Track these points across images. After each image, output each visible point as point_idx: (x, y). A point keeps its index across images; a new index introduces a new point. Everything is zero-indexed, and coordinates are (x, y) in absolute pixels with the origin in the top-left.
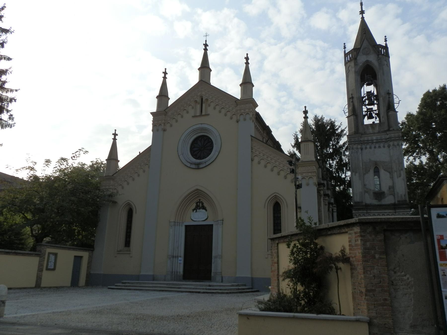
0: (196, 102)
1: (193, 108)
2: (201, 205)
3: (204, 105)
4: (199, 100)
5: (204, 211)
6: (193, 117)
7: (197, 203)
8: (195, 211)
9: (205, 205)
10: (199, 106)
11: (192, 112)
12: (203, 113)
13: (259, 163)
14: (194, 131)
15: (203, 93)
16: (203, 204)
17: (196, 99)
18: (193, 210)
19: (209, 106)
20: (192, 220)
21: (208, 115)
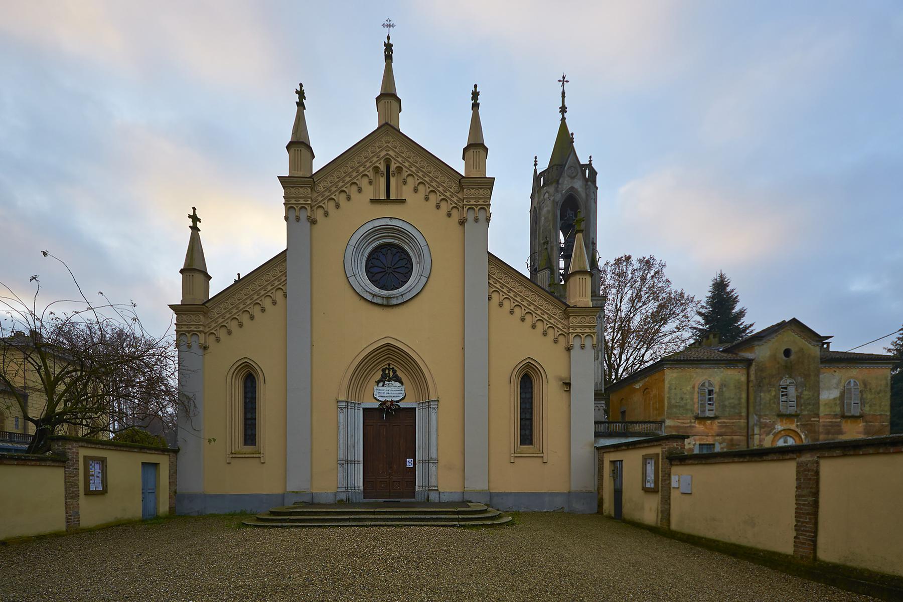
0: (376, 169)
1: (371, 183)
2: (391, 374)
3: (393, 181)
4: (382, 168)
5: (398, 384)
6: (373, 201)
7: (384, 371)
8: (381, 384)
9: (399, 373)
10: (383, 181)
11: (369, 192)
12: (393, 197)
13: (501, 305)
14: (376, 230)
15: (391, 153)
16: (394, 372)
17: (377, 164)
18: (378, 383)
19: (405, 182)
20: (376, 399)
21: (403, 201)
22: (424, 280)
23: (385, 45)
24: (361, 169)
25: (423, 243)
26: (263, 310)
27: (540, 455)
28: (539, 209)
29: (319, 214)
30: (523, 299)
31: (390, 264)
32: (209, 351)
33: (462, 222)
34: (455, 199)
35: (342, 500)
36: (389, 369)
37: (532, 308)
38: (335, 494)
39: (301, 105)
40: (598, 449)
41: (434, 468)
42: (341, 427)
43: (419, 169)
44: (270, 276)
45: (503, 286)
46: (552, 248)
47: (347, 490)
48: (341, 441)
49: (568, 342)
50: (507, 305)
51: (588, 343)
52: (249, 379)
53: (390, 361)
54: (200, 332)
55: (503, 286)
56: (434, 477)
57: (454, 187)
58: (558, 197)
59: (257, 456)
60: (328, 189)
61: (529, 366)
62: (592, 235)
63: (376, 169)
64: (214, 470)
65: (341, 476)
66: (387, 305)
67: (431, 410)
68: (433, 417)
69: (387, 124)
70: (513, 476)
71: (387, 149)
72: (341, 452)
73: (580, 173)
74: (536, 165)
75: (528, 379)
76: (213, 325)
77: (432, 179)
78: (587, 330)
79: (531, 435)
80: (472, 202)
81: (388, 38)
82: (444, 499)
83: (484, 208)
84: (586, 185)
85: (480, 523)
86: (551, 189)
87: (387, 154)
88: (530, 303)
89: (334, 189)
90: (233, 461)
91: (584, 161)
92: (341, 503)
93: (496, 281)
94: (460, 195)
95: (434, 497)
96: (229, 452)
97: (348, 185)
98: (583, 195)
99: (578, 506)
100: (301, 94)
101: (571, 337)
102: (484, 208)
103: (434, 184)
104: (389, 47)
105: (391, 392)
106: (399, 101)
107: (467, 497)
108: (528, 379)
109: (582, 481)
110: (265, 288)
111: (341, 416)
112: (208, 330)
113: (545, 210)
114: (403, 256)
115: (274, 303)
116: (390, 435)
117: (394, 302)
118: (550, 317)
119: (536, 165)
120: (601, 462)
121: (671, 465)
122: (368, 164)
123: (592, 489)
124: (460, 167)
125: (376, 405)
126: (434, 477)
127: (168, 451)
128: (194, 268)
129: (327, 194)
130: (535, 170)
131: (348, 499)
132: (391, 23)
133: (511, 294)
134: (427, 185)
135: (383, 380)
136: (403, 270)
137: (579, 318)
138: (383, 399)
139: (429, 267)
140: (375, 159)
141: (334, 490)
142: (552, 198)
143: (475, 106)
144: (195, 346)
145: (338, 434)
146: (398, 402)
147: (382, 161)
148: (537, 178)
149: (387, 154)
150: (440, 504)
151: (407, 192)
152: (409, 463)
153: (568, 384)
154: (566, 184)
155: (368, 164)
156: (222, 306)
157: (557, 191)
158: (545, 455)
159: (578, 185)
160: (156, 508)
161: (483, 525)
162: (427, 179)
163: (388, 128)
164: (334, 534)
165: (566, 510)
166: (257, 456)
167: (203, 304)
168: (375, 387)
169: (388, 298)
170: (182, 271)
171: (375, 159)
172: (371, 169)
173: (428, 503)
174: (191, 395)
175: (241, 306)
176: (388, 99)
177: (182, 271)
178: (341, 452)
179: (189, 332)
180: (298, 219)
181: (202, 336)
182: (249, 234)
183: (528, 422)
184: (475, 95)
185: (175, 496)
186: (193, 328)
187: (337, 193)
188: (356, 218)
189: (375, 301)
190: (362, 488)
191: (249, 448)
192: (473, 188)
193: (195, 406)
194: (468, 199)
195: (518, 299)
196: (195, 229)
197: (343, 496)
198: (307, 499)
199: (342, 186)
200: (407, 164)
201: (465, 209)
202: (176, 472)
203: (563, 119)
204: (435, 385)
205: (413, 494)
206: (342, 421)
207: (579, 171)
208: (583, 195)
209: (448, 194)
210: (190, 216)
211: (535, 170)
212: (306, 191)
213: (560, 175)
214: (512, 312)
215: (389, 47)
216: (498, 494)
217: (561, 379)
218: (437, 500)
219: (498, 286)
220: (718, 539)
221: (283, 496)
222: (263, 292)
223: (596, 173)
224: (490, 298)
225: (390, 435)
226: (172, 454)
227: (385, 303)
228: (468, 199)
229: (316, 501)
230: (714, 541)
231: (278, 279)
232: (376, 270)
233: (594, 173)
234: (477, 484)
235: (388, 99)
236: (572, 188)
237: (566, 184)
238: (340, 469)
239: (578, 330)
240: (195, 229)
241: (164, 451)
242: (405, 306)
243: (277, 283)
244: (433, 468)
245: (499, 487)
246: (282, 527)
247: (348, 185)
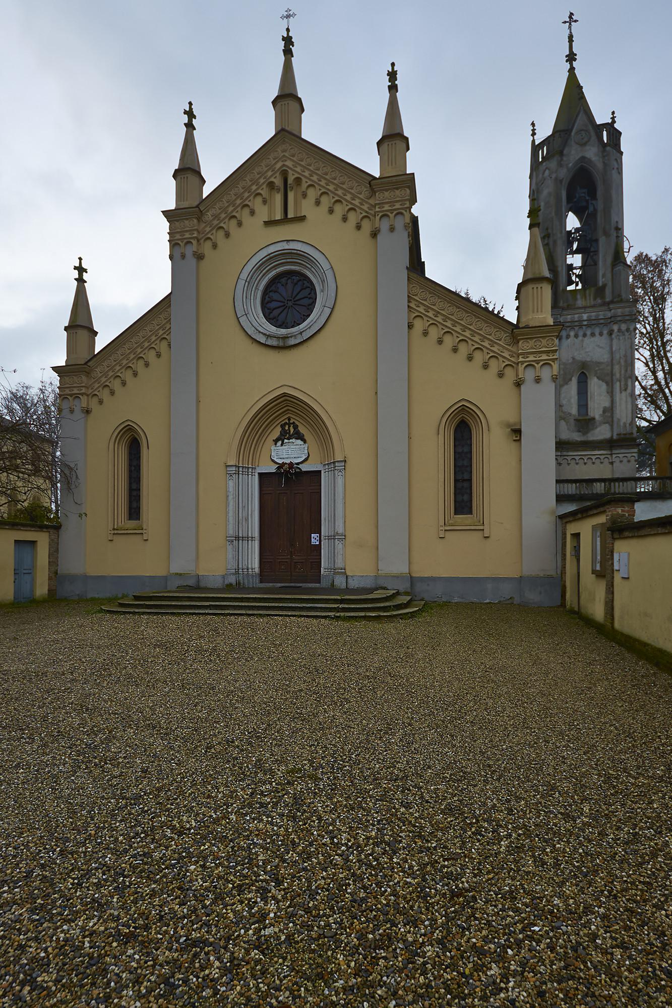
0: (271, 185)
1: (265, 202)
2: (292, 430)
3: (291, 195)
4: (278, 181)
5: (299, 442)
6: (268, 223)
7: (283, 426)
8: (280, 442)
9: (302, 429)
10: (278, 198)
11: (263, 213)
12: (291, 215)
14: (271, 258)
15: (289, 163)
16: (296, 427)
17: (272, 179)
18: (276, 441)
19: (305, 195)
20: (273, 461)
21: (302, 219)
22: (328, 311)
23: (284, 39)
24: (254, 187)
25: (326, 266)
26: (147, 365)
27: (479, 528)
28: (538, 192)
29: (207, 247)
30: (455, 323)
31: (289, 295)
32: (92, 415)
33: (374, 234)
34: (365, 207)
35: (231, 584)
36: (289, 424)
37: (467, 333)
38: (223, 577)
39: (190, 126)
40: (561, 517)
41: (340, 545)
42: (231, 497)
43: (321, 178)
44: (155, 323)
45: (427, 309)
46: (555, 242)
47: (237, 573)
48: (231, 514)
49: (517, 375)
50: (434, 333)
51: (546, 374)
52: (133, 444)
53: (287, 415)
54: (82, 394)
55: (427, 309)
56: (340, 557)
57: (365, 191)
58: (563, 173)
59: (139, 532)
60: (216, 217)
61: (463, 409)
62: (614, 218)
63: (271, 185)
64: (98, 550)
65: (231, 556)
66: (283, 346)
67: (336, 472)
68: (340, 481)
69: (283, 130)
70: (447, 556)
71: (284, 158)
72: (231, 527)
73: (594, 137)
74: (534, 134)
75: (463, 428)
76: (97, 385)
77: (337, 187)
78: (544, 357)
79: (471, 501)
80: (387, 207)
81: (288, 30)
82: (353, 584)
83: (402, 214)
84: (604, 151)
85: (363, 614)
86: (553, 164)
87: (288, 164)
88: (465, 328)
89: (223, 216)
90: (115, 538)
91: (601, 118)
92: (229, 587)
93: (419, 304)
94: (372, 201)
95: (340, 582)
96: (111, 527)
97: (239, 209)
98: (600, 165)
99: (533, 596)
100: (190, 114)
101: (521, 368)
102: (402, 214)
103: (340, 192)
104: (288, 41)
105: (291, 453)
106: (299, 100)
107: (381, 583)
108: (463, 428)
109: (536, 561)
110: (148, 339)
111: (231, 484)
112: (90, 391)
113: (545, 192)
114: (306, 284)
115: (159, 355)
116: (291, 502)
117: (292, 342)
118: (493, 344)
119: (534, 134)
120: (564, 534)
121: (614, 539)
122: (262, 181)
123: (553, 573)
124: (372, 165)
125: (272, 469)
126: (340, 557)
127: (47, 527)
128: (80, 324)
129: (215, 222)
130: (533, 141)
131: (238, 583)
132: (291, 13)
133: (439, 319)
134: (331, 195)
135: (281, 439)
136: (306, 302)
137: (532, 343)
138: (280, 461)
139: (333, 295)
140: (270, 173)
141: (221, 572)
142: (554, 176)
143: (393, 88)
144: (77, 410)
145: (227, 505)
146: (298, 464)
147: (277, 174)
148: (535, 148)
149: (288, 164)
150: (348, 590)
151: (307, 208)
152: (314, 539)
153: (517, 432)
154: (573, 154)
155: (262, 181)
156: (105, 364)
157: (560, 165)
158: (486, 527)
159: (592, 153)
160: (32, 590)
161: (364, 617)
162: (331, 187)
163: (287, 134)
164: (173, 622)
165: (517, 600)
166: (139, 532)
167: (86, 364)
168: (273, 448)
169: (285, 338)
170: (66, 329)
171: (270, 173)
172: (264, 186)
173: (332, 589)
174: (72, 465)
175: (125, 362)
176: (288, 101)
177: (66, 329)
178: (231, 527)
179: (71, 395)
180: (183, 256)
181: (84, 399)
182: (134, 278)
183: (466, 485)
184: (392, 75)
185: (55, 576)
186: (76, 391)
187: (226, 220)
188: (252, 243)
189: (269, 342)
190: (257, 570)
191: (133, 523)
192: (386, 190)
193: (77, 477)
194: (381, 204)
195: (449, 324)
196: (81, 281)
197: (232, 580)
198: (191, 582)
199: (232, 212)
200: (307, 174)
201: (378, 218)
202: (57, 551)
203: (572, 70)
204: (341, 440)
205: (318, 578)
206: (231, 489)
207: (593, 133)
208: (600, 165)
209: (357, 202)
210: (75, 268)
211: (533, 141)
212: (195, 221)
213: (565, 143)
214: (440, 342)
215: (288, 41)
216: (423, 580)
217: (508, 425)
218: (344, 586)
219: (421, 309)
220: (649, 642)
221: (165, 578)
222: (146, 344)
223: (620, 133)
224: (410, 326)
225: (291, 502)
226: (52, 531)
227: (281, 344)
228: (381, 204)
229: (202, 584)
230: (645, 644)
231: (162, 327)
232: (273, 305)
233: (615, 135)
234: (395, 565)
235: (288, 101)
236: (583, 158)
237: (573, 154)
238: (230, 548)
239: (531, 358)
240: (81, 281)
241: (42, 528)
242: (305, 345)
243: (161, 332)
244: (339, 546)
245: (422, 570)
246: (134, 613)
247: (239, 209)
